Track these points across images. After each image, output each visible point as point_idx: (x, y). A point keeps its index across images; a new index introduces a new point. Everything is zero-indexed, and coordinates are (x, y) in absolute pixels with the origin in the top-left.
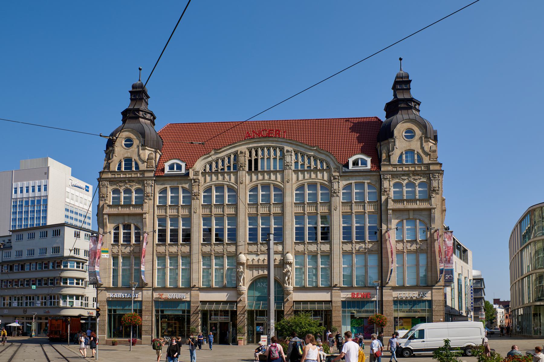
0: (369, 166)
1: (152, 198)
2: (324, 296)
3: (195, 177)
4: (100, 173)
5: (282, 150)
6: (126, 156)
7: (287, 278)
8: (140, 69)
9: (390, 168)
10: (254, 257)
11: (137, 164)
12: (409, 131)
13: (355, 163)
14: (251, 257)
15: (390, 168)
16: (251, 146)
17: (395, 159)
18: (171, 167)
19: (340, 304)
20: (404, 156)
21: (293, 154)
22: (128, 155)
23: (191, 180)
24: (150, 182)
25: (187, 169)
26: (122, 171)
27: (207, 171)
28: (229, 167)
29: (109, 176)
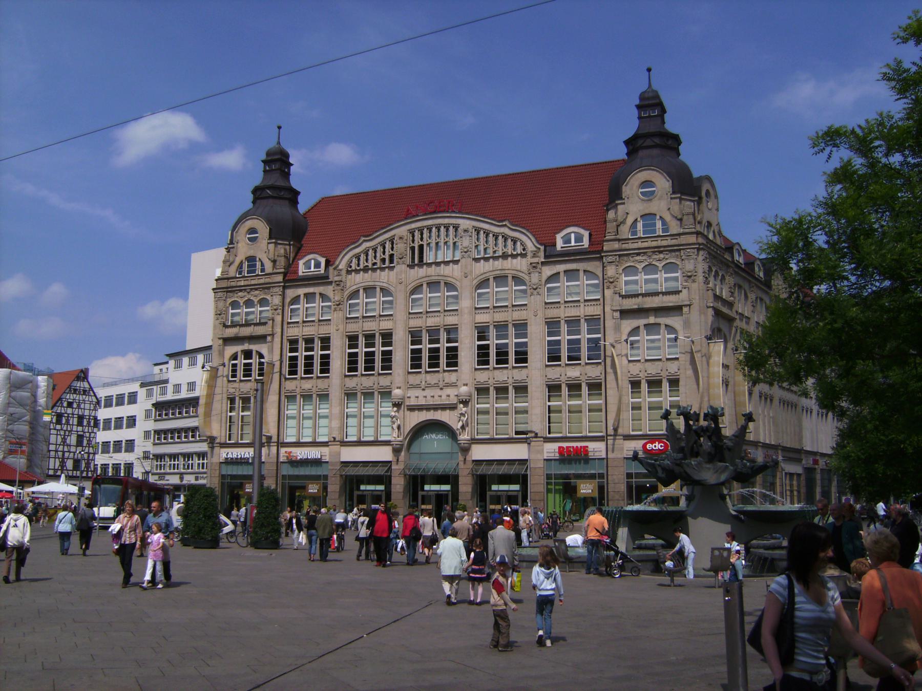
0: (586, 243)
1: (280, 311)
2: (517, 452)
3: (337, 279)
5: (456, 228)
7: (460, 424)
8: (279, 128)
9: (616, 245)
10: (418, 392)
11: (262, 265)
12: (647, 183)
13: (567, 240)
14: (412, 393)
15: (616, 245)
16: (413, 226)
17: (625, 232)
19: (541, 464)
20: (640, 226)
21: (474, 234)
22: (251, 253)
23: (331, 283)
26: (244, 277)
27: (353, 268)
28: (383, 260)
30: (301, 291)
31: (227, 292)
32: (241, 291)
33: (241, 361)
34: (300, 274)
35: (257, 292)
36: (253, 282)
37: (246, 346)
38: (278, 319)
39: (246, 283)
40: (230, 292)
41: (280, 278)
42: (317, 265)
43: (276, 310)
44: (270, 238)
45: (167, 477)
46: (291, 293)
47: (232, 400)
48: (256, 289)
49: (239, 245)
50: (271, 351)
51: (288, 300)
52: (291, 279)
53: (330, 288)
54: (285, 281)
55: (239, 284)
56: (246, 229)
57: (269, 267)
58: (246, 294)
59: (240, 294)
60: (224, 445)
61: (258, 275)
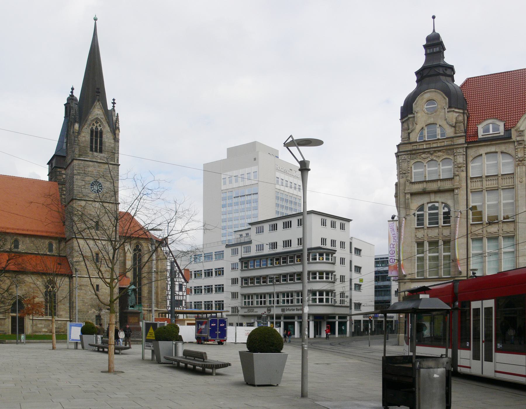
1: (464, 169)
4: (398, 146)
6: (429, 122)
18: (486, 130)
24: (461, 150)
25: (507, 130)
29: (409, 148)
30: (483, 151)
31: (410, 154)
32: (424, 153)
33: (427, 212)
34: (480, 136)
35: (440, 154)
36: (435, 145)
37: (433, 198)
38: (464, 174)
39: (428, 146)
40: (414, 154)
41: (462, 141)
42: (496, 128)
43: (461, 167)
44: (450, 107)
45: (255, 310)
46: (472, 152)
47: (420, 244)
48: (439, 151)
49: (419, 115)
50: (456, 202)
51: (470, 159)
52: (473, 141)
53: (512, 146)
54: (466, 142)
55: (421, 147)
56: (425, 100)
57: (450, 132)
58: (428, 155)
59: (423, 156)
60: (413, 280)
61: (439, 139)
